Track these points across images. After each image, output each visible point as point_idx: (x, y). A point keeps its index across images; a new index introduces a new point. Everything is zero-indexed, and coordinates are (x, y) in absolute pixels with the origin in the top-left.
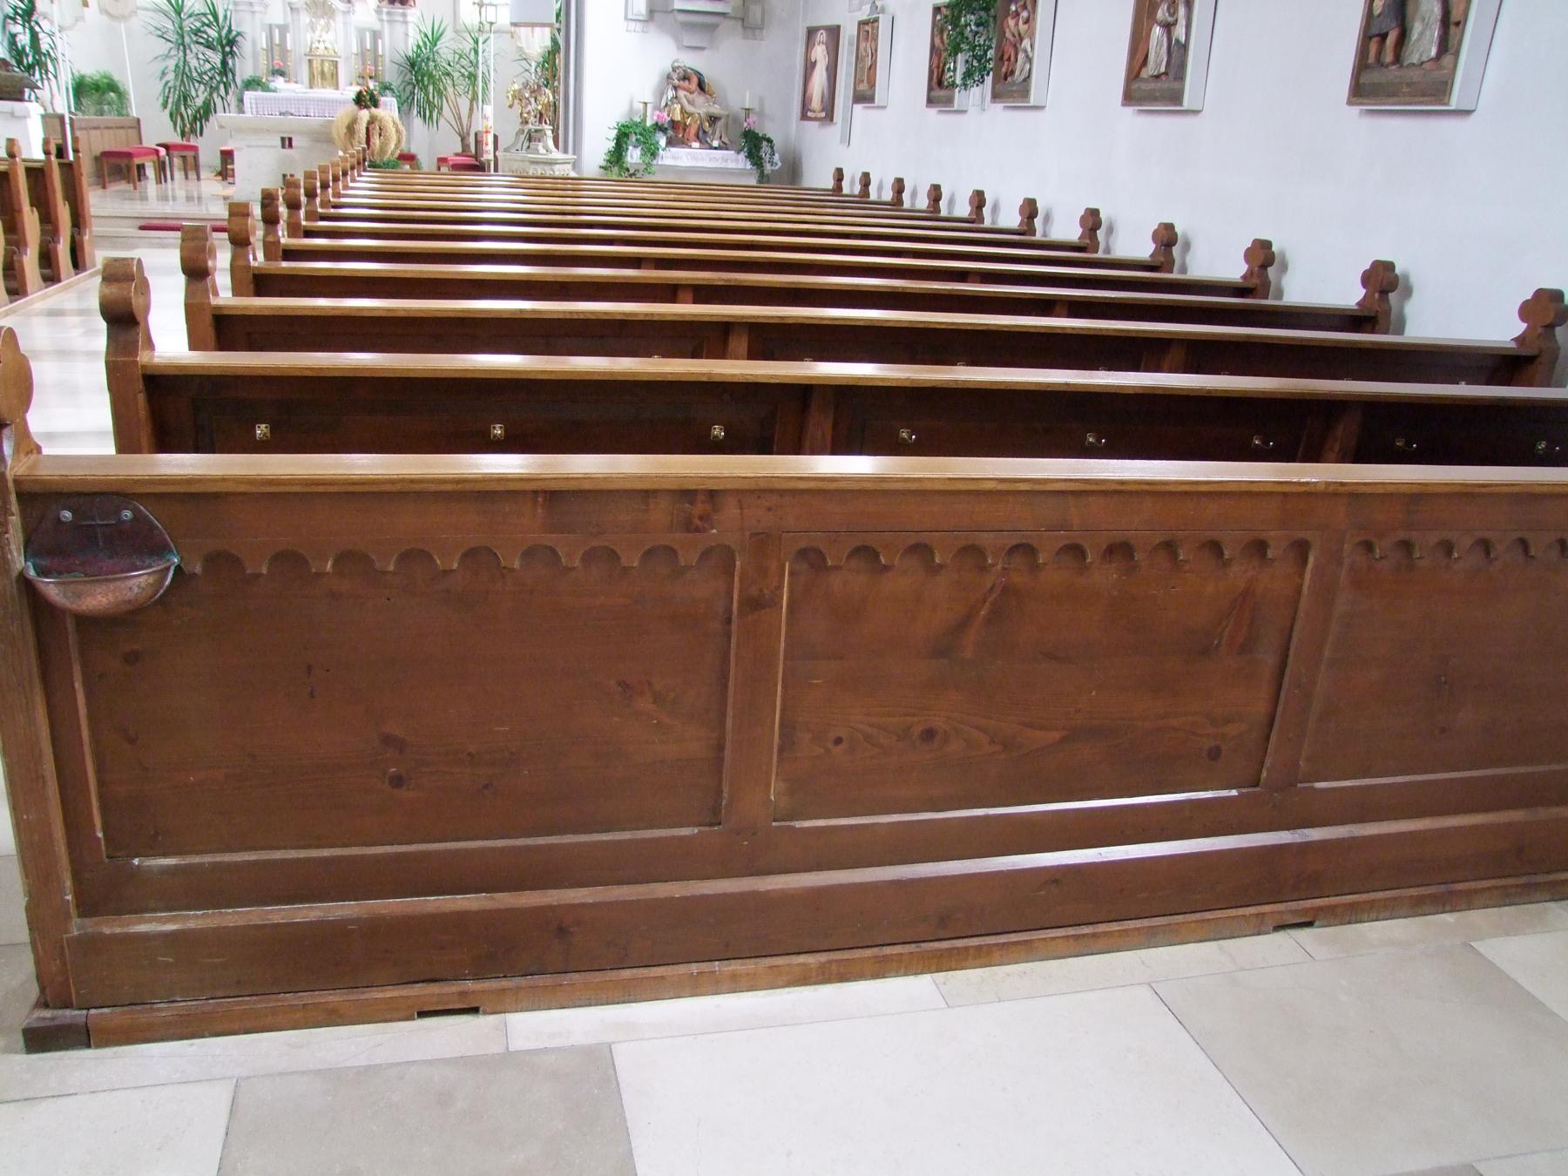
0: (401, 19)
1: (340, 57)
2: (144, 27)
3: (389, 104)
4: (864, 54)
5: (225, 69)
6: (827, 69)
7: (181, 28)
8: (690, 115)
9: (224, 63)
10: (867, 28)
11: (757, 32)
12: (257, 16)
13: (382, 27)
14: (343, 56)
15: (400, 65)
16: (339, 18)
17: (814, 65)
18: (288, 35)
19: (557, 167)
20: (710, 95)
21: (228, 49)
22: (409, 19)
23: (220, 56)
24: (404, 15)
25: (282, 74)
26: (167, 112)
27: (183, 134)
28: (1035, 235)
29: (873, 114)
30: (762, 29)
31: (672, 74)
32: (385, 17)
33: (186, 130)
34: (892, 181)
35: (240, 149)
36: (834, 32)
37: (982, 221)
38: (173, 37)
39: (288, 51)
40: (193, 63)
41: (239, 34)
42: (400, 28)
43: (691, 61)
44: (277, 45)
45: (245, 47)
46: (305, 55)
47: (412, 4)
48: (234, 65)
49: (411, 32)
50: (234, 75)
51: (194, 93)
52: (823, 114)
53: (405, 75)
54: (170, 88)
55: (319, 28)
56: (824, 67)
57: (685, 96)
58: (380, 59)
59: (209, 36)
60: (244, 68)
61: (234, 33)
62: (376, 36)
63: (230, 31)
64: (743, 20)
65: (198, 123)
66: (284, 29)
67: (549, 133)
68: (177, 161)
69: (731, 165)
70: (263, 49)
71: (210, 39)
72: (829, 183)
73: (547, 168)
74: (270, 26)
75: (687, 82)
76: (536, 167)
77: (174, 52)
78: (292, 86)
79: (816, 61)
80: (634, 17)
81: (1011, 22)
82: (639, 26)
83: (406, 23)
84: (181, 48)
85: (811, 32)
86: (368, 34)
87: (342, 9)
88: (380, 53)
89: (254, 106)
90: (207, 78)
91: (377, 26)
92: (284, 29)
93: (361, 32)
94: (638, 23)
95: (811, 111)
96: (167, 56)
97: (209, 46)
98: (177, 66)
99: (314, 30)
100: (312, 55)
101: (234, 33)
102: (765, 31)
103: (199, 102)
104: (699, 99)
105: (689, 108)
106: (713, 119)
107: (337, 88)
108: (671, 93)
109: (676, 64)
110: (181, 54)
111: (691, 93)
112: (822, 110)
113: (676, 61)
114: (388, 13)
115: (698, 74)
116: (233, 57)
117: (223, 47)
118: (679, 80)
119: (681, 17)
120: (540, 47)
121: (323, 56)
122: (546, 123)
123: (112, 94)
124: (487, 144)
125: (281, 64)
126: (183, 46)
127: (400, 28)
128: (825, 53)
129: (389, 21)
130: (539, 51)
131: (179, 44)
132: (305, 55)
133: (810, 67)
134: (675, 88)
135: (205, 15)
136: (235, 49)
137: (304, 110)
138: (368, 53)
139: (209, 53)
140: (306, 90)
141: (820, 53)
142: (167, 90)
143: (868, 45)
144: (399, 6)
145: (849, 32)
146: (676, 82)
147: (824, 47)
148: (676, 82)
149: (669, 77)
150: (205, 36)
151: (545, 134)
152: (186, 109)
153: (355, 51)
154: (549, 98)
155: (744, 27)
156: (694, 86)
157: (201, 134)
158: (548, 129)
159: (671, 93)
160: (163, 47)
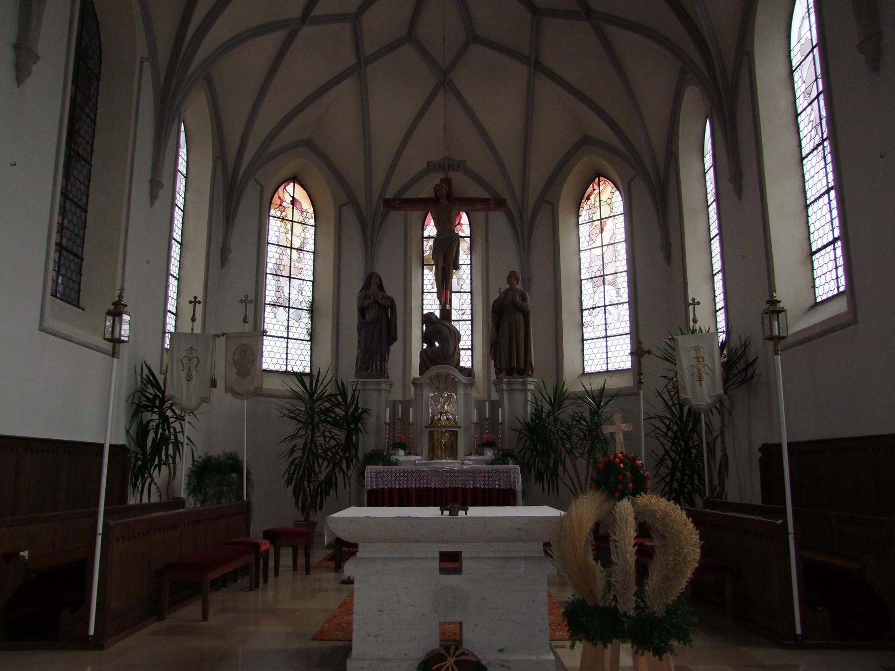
0: (520, 387)
1: (460, 427)
2: (278, 410)
3: (512, 471)
5: (350, 446)
7: (312, 408)
9: (348, 439)
12: (383, 393)
13: (501, 397)
14: (463, 427)
15: (520, 432)
16: (461, 391)
18: (411, 409)
21: (353, 426)
22: (530, 387)
23: (345, 432)
24: (524, 383)
25: (403, 446)
26: (291, 487)
32: (505, 387)
33: (307, 504)
38: (303, 417)
39: (410, 424)
40: (320, 440)
41: (365, 411)
42: (519, 397)
44: (399, 419)
45: (371, 422)
47: (530, 373)
48: (358, 439)
49: (529, 398)
50: (357, 450)
51: (317, 468)
53: (526, 441)
54: (296, 465)
59: (337, 415)
60: (368, 443)
61: (360, 410)
62: (495, 405)
63: (357, 408)
65: (319, 498)
66: (406, 404)
68: (286, 559)
71: (338, 418)
74: (394, 402)
77: (302, 432)
78: (413, 458)
83: (525, 390)
84: (310, 427)
88: (500, 421)
89: (374, 480)
90: (330, 453)
91: (495, 396)
92: (406, 404)
96: (295, 436)
97: (336, 424)
98: (305, 444)
100: (434, 427)
101: (360, 410)
103: (322, 477)
107: (453, 455)
110: (309, 432)
114: (508, 383)
116: (357, 433)
120: (711, 397)
121: (444, 427)
123: (234, 475)
125: (404, 437)
127: (519, 397)
129: (510, 391)
130: (709, 401)
131: (308, 424)
132: (426, 427)
135: (333, 395)
136: (359, 425)
137: (425, 482)
139: (335, 431)
140: (425, 461)
142: (293, 467)
144: (518, 376)
150: (333, 415)
152: (309, 484)
157: (321, 508)
160: (291, 427)
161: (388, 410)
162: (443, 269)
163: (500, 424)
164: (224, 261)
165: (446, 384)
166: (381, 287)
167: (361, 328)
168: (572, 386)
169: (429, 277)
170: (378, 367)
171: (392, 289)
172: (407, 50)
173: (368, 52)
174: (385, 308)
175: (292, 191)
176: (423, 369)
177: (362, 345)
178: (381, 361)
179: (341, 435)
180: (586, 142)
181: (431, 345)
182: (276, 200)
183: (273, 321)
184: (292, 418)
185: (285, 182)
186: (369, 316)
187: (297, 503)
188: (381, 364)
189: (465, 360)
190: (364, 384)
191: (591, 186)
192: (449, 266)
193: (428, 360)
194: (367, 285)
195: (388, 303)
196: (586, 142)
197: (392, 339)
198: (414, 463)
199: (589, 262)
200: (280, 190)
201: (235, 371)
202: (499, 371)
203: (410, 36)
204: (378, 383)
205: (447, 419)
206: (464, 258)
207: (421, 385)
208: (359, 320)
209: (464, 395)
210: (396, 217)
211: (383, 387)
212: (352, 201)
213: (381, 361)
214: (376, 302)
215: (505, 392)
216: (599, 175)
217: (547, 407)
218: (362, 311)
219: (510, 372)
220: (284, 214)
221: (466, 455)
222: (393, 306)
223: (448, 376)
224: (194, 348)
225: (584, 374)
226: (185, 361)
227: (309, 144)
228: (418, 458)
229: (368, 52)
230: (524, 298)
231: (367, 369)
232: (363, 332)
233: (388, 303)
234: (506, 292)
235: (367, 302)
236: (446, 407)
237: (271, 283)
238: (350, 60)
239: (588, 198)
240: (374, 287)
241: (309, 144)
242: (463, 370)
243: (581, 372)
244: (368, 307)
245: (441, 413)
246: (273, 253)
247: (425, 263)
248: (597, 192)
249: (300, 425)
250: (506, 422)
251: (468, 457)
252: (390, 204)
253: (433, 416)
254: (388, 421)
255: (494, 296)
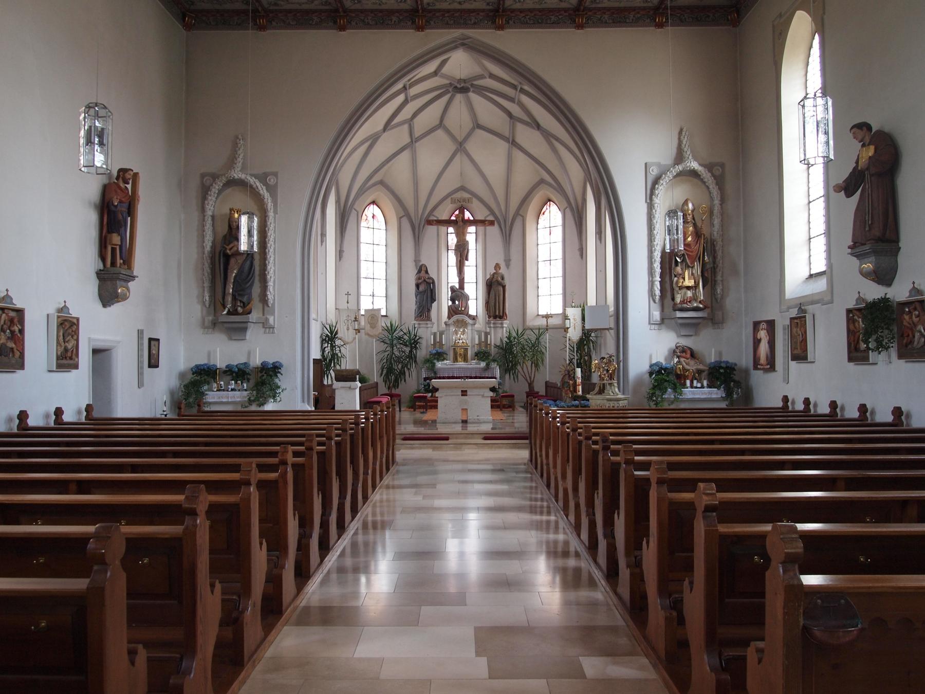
1: (469, 346)
4: (796, 334)
6: (769, 343)
8: (688, 370)
9: (411, 351)
10: (796, 321)
11: (720, 325)
12: (429, 329)
13: (490, 330)
16: (470, 328)
17: (760, 341)
18: (443, 336)
19: (621, 402)
20: (697, 359)
22: (505, 325)
24: (502, 324)
27: (389, 388)
28: (868, 421)
29: (803, 366)
30: (722, 323)
31: (676, 350)
32: (492, 326)
34: (803, 399)
35: (441, 397)
36: (771, 324)
37: (902, 425)
39: (443, 345)
43: (684, 342)
45: (423, 343)
46: (452, 346)
48: (416, 353)
52: (769, 366)
55: (460, 333)
56: (767, 342)
57: (684, 361)
58: (489, 346)
61: (418, 337)
62: (487, 334)
64: (712, 319)
67: (616, 385)
69: (714, 396)
70: (432, 345)
72: (780, 404)
73: (615, 403)
75: (684, 354)
76: (610, 402)
79: (761, 339)
80: (654, 323)
81: (906, 317)
82: (656, 327)
85: (756, 325)
86: (483, 333)
87: (471, 323)
88: (489, 343)
90: (402, 360)
91: (488, 330)
92: (441, 333)
93: (479, 333)
94: (656, 325)
95: (760, 365)
97: (406, 346)
99: (457, 334)
101: (418, 337)
102: (724, 324)
104: (692, 362)
105: (687, 367)
106: (700, 372)
108: (676, 360)
109: (678, 345)
111: (687, 359)
112: (767, 365)
113: (678, 343)
114: (494, 323)
115: (690, 348)
117: (411, 344)
118: (680, 353)
119: (680, 321)
121: (461, 346)
122: (614, 380)
124: (579, 391)
126: (392, 346)
128: (767, 334)
129: (494, 327)
133: (757, 342)
134: (678, 357)
138: (483, 344)
139: (404, 348)
141: (763, 334)
143: (799, 329)
144: (499, 319)
145: (782, 323)
146: (679, 354)
147: (765, 331)
148: (679, 354)
149: (674, 352)
151: (614, 385)
153: (477, 342)
154: (615, 366)
155: (712, 323)
156: (688, 355)
157: (398, 388)
158: (615, 382)
159: (676, 360)
160: (383, 347)
161: (432, 336)
162: (460, 261)
163: (489, 344)
164: (340, 258)
165: (462, 324)
166: (427, 272)
167: (417, 295)
168: (532, 322)
169: (452, 258)
170: (427, 315)
171: (433, 274)
172: (440, 133)
173: (417, 134)
174: (429, 284)
175: (373, 210)
176: (449, 318)
177: (418, 304)
178: (428, 312)
179: (407, 350)
180: (542, 181)
181: (453, 302)
182: (364, 217)
183: (366, 287)
184: (382, 342)
185: (368, 205)
186: (422, 288)
187: (385, 386)
188: (428, 314)
189: (472, 312)
190: (419, 324)
191: (545, 206)
192: (463, 259)
193: (453, 311)
194: (419, 271)
195: (431, 281)
196: (542, 181)
197: (433, 300)
198: (446, 364)
199: (543, 254)
200: (366, 210)
201: (369, 326)
202: (489, 317)
203: (441, 125)
204: (427, 324)
205: (463, 342)
206: (472, 255)
207: (449, 325)
208: (416, 291)
209: (471, 329)
210: (432, 229)
211: (429, 326)
212: (407, 215)
213: (428, 312)
214: (425, 280)
215: (492, 328)
216: (550, 200)
217: (514, 334)
218: (417, 286)
219: (495, 317)
220: (369, 224)
221: (472, 360)
222: (433, 283)
223: (463, 320)
224: (350, 315)
225: (538, 315)
226: (346, 321)
227: (381, 183)
228: (448, 362)
229: (417, 134)
230: (503, 279)
231: (421, 316)
232: (418, 297)
233: (431, 281)
234: (494, 273)
235: (420, 281)
236: (462, 336)
237: (363, 265)
238: (407, 140)
239: (543, 214)
240: (423, 272)
241: (381, 183)
242: (470, 316)
243: (537, 314)
244: (421, 283)
245: (459, 339)
246: (363, 248)
247: (449, 249)
248: (548, 211)
249: (386, 345)
250: (493, 344)
251: (473, 361)
252: (429, 223)
253: (456, 341)
254: (432, 343)
255: (488, 277)
